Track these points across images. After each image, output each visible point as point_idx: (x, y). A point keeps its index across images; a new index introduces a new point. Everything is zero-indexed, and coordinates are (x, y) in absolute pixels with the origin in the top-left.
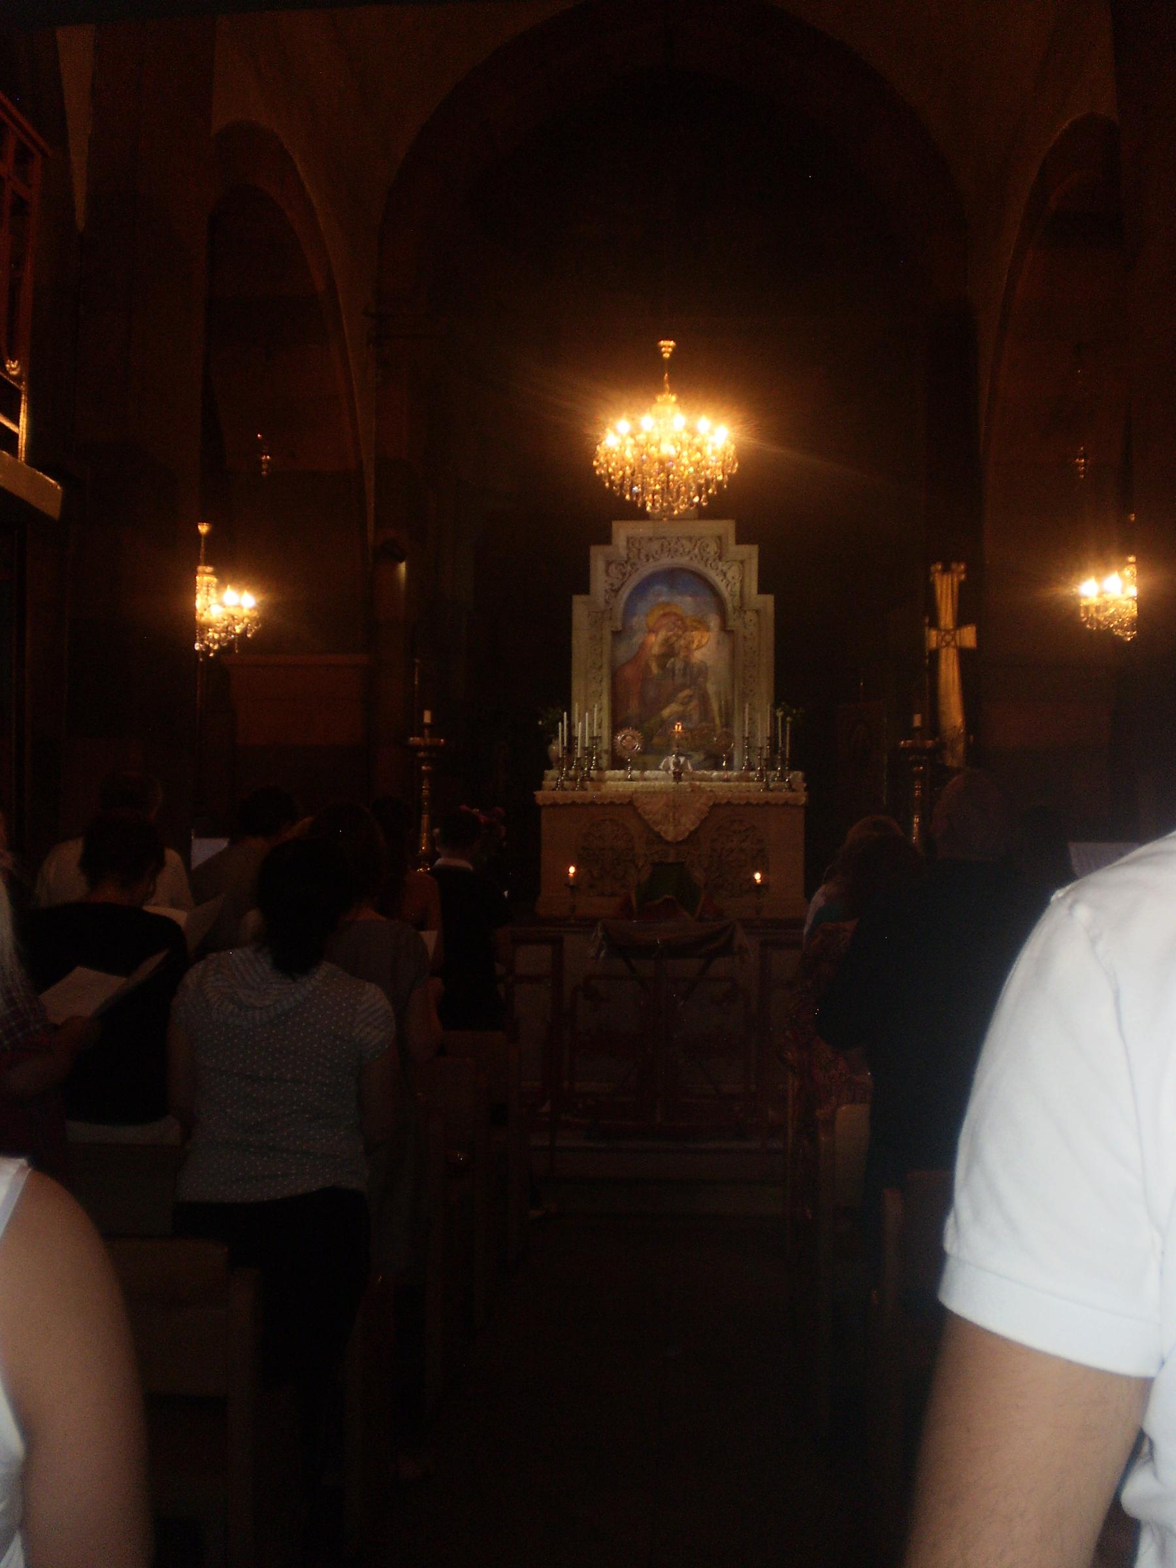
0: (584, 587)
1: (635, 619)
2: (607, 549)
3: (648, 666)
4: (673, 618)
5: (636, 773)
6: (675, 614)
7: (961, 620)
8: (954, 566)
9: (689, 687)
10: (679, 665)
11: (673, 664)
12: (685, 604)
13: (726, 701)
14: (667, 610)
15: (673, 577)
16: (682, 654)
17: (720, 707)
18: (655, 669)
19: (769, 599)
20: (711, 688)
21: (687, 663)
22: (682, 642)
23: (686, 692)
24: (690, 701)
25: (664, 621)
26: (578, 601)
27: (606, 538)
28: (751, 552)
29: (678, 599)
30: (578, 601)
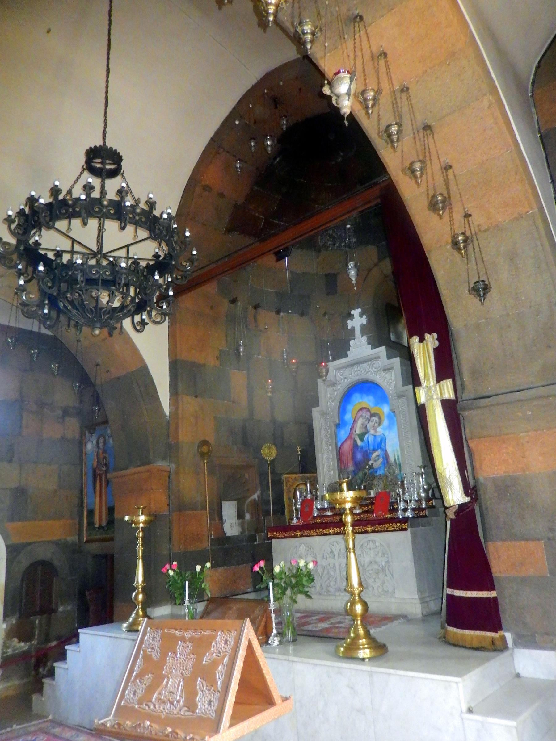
0: (316, 403)
3: (355, 441)
4: (364, 411)
6: (365, 408)
7: (440, 378)
8: (427, 336)
9: (377, 450)
10: (371, 439)
11: (368, 438)
12: (368, 401)
13: (398, 456)
16: (372, 432)
18: (359, 443)
22: (370, 422)
24: (378, 459)
25: (360, 413)
26: (316, 412)
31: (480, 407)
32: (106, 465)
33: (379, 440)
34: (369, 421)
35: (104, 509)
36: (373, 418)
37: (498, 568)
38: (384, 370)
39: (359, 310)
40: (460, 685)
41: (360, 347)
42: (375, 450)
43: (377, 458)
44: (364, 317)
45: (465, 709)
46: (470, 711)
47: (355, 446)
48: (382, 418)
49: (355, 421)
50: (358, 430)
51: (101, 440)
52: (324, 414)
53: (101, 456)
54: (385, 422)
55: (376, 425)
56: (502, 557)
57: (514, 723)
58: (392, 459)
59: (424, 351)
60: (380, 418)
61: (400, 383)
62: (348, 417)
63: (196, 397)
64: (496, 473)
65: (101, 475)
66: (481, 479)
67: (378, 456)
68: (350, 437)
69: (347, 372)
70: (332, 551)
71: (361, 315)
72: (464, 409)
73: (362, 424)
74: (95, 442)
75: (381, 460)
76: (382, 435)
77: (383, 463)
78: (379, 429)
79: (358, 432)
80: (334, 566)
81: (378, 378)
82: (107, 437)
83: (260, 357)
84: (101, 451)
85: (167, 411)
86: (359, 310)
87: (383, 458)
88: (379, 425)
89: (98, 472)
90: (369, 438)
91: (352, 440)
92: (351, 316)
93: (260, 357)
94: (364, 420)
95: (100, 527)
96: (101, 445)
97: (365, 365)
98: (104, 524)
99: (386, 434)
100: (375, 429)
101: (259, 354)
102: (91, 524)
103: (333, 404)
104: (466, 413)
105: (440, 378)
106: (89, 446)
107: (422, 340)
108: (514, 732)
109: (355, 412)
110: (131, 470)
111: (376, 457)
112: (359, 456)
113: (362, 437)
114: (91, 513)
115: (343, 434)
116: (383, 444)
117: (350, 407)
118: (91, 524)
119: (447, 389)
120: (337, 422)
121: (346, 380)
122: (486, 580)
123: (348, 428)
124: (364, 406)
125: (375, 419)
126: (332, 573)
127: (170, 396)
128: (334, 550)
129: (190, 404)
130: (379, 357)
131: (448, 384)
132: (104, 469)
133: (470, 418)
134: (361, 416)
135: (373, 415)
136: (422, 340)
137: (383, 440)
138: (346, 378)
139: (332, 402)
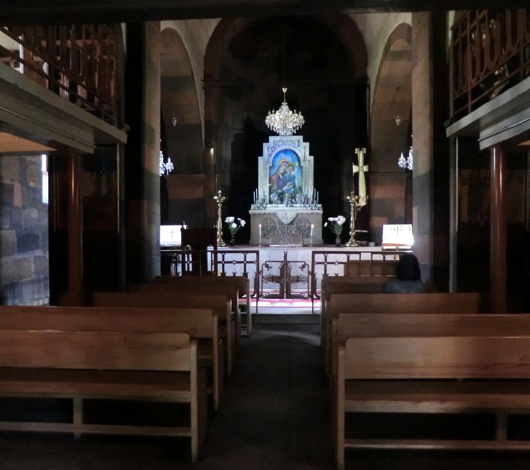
0: (261, 155)
3: (279, 176)
5: (276, 205)
10: (287, 176)
12: (289, 158)
15: (286, 151)
16: (288, 173)
18: (281, 177)
19: (312, 157)
20: (296, 182)
21: (290, 176)
23: (290, 183)
25: (284, 163)
26: (260, 158)
27: (267, 141)
28: (307, 144)
29: (287, 157)
30: (260, 158)
42: (289, 181)
47: (279, 177)
48: (295, 167)
49: (280, 167)
50: (281, 171)
60: (293, 167)
68: (276, 174)
75: (292, 186)
88: (293, 170)
90: (287, 175)
100: (290, 172)
105: (365, 163)
109: (280, 163)
112: (280, 183)
113: (283, 174)
115: (274, 171)
117: (277, 160)
119: (366, 169)
123: (276, 169)
124: (286, 160)
125: (292, 167)
134: (284, 165)
135: (290, 165)
137: (294, 177)
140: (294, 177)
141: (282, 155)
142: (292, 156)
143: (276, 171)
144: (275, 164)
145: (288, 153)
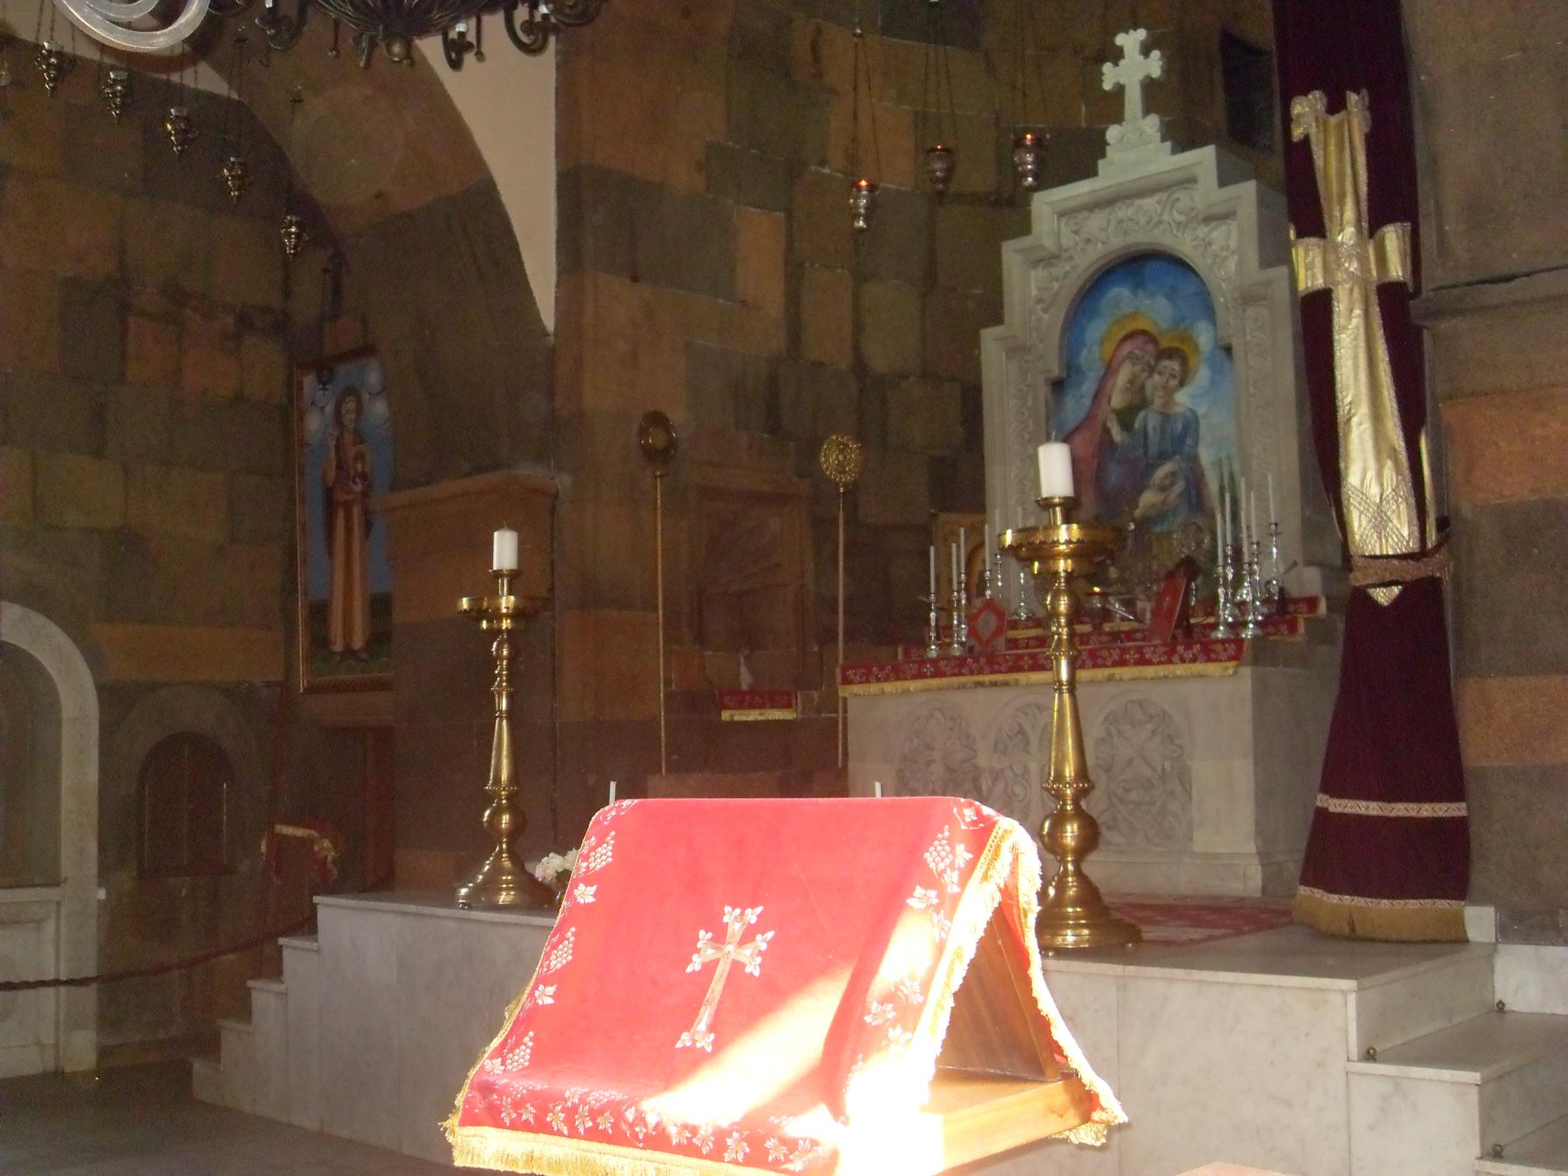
0: (994, 313)
1: (1084, 353)
2: (1025, 241)
3: (1107, 431)
4: (1140, 340)
6: (1143, 333)
12: (1155, 309)
14: (1130, 328)
15: (1137, 265)
16: (1158, 403)
17: (1222, 488)
18: (1117, 434)
20: (1206, 455)
21: (1166, 417)
22: (1156, 378)
23: (1167, 468)
24: (1173, 484)
25: (1127, 348)
26: (989, 336)
30: (989, 336)
31: (1481, 309)
32: (364, 476)
33: (1179, 427)
34: (1151, 370)
35: (358, 603)
36: (1166, 363)
37: (1480, 746)
38: (1208, 220)
39: (1141, 34)
40: (1352, 998)
41: (1137, 147)
42: (1163, 457)
43: (1167, 482)
44: (1156, 54)
45: (1354, 1051)
46: (1370, 1056)
48: (1193, 361)
49: (1110, 370)
50: (1117, 399)
51: (350, 404)
52: (1016, 350)
53: (351, 451)
54: (1202, 376)
55: (1173, 383)
56: (1497, 716)
57: (1475, 1077)
58: (1213, 486)
59: (1335, 138)
60: (1184, 362)
61: (1253, 258)
62: (1091, 357)
63: (635, 279)
64: (1507, 493)
65: (348, 506)
66: (1466, 511)
67: (1173, 474)
68: (1089, 418)
69: (1095, 223)
70: (1021, 731)
71: (1146, 50)
72: (1439, 314)
73: (1131, 382)
74: (329, 409)
75: (1179, 486)
76: (1189, 414)
77: (1185, 493)
78: (1182, 398)
79: (1117, 400)
80: (1026, 770)
81: (1185, 245)
82: (366, 396)
83: (827, 171)
84: (348, 437)
85: (549, 320)
86: (1141, 34)
87: (1187, 479)
88: (1182, 384)
89: (341, 496)
90: (1149, 420)
91: (1099, 428)
92: (1117, 55)
93: (827, 171)
94: (1138, 367)
95: (349, 652)
96: (349, 418)
97: (1149, 203)
98: (358, 643)
99: (1201, 411)
100: (1169, 393)
101: (823, 162)
102: (320, 642)
103: (1046, 316)
104: (1444, 325)
106: (314, 424)
107: (1336, 105)
108: (1474, 1095)
109: (1109, 347)
110: (446, 487)
111: (1166, 477)
112: (1114, 475)
113: (1126, 417)
114: (319, 612)
116: (1189, 441)
117: (1096, 330)
118: (320, 642)
120: (1056, 371)
121: (1090, 248)
122: (1449, 779)
123: (1088, 387)
124: (1141, 324)
125: (1174, 365)
126: (1018, 790)
127: (560, 274)
128: (1028, 729)
129: (619, 301)
130: (1192, 180)
131: (1393, 238)
132: (358, 488)
133: (1452, 343)
134: (1131, 356)
136: (1336, 105)
137: (1191, 425)
138: (1088, 241)
139: (1045, 310)
140: (1191, 425)
141: (1120, 294)
142: (1171, 295)
143: (1087, 402)
144: (1084, 357)
145: (1152, 268)
